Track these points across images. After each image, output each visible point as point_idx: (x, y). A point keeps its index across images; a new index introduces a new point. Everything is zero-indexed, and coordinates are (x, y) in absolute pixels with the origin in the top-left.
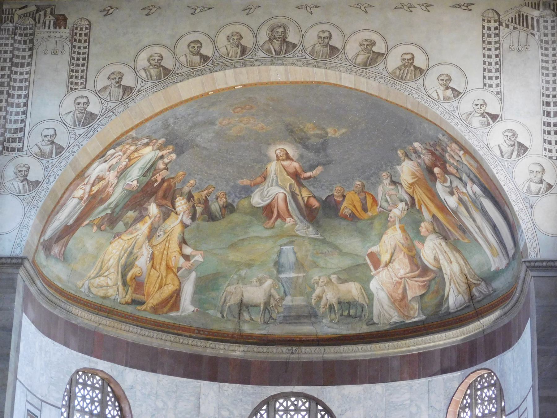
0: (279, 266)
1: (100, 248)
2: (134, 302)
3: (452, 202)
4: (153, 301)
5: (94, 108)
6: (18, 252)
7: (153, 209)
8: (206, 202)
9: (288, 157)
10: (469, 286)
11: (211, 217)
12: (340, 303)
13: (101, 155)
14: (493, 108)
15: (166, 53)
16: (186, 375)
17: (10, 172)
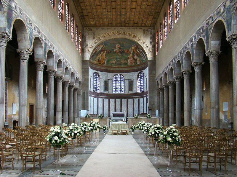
0: (117, 59)
1: (96, 57)
2: (100, 64)
3: (138, 52)
4: (102, 63)
6: (89, 59)
7: (102, 52)
8: (108, 51)
9: (118, 46)
10: (140, 61)
11: (109, 53)
12: (124, 63)
13: (97, 47)
15: (105, 35)
17: (87, 50)
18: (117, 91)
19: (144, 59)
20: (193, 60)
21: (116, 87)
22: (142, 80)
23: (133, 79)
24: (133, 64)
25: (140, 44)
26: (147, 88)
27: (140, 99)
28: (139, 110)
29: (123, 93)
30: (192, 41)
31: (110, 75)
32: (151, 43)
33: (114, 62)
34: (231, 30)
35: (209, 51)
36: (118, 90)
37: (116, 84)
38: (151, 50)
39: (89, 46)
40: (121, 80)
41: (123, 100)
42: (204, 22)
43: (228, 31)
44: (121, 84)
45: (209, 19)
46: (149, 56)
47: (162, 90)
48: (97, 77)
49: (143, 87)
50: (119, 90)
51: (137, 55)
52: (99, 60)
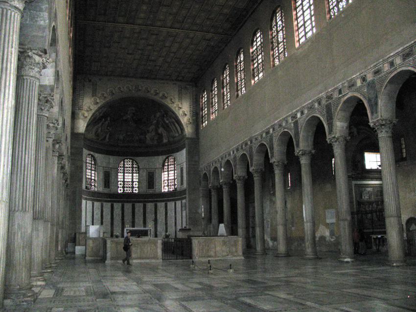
3: (167, 122)
4: (100, 139)
5: (98, 101)
7: (104, 120)
14: (180, 106)
16: (107, 154)
17: (80, 114)
18: (126, 189)
19: (177, 135)
20: (298, 145)
21: (124, 182)
22: (172, 170)
23: (156, 167)
24: (155, 142)
25: (174, 110)
26: (182, 184)
27: (168, 203)
28: (166, 224)
29: (137, 192)
30: (294, 117)
31: (112, 159)
32: (191, 109)
33: (121, 137)
34: (376, 113)
35: (333, 136)
36: (127, 187)
37: (124, 176)
38: (190, 121)
39: (85, 107)
40: (133, 170)
41: (137, 205)
42: (323, 93)
43: (372, 113)
44: (132, 176)
45: (333, 91)
46: (188, 130)
47: (219, 190)
48: (91, 164)
49: (174, 182)
50: (129, 187)
51: (164, 127)
52: (97, 131)
